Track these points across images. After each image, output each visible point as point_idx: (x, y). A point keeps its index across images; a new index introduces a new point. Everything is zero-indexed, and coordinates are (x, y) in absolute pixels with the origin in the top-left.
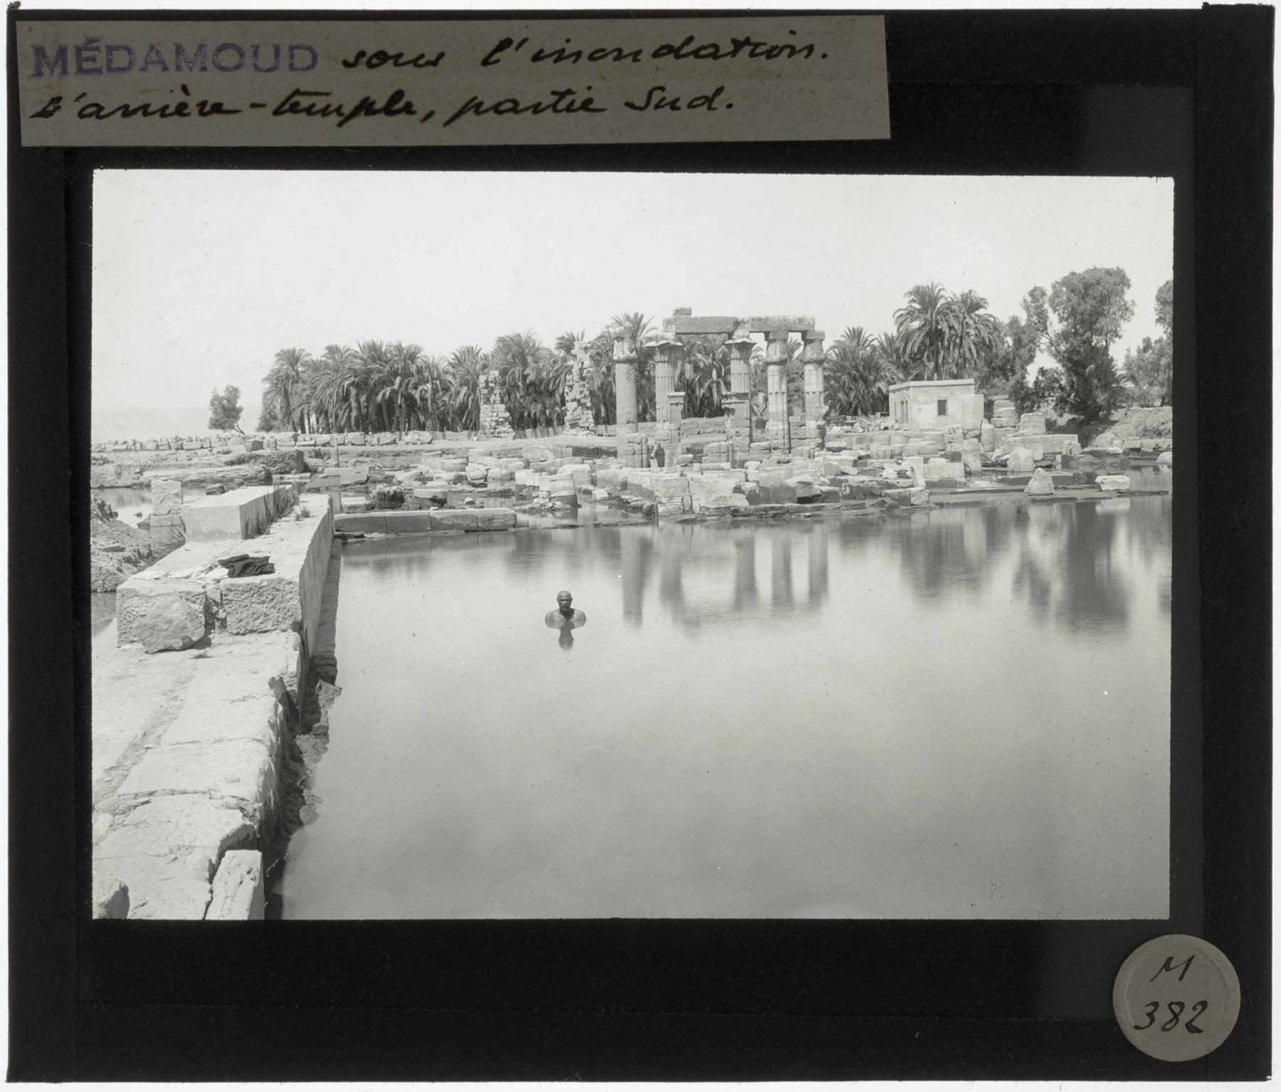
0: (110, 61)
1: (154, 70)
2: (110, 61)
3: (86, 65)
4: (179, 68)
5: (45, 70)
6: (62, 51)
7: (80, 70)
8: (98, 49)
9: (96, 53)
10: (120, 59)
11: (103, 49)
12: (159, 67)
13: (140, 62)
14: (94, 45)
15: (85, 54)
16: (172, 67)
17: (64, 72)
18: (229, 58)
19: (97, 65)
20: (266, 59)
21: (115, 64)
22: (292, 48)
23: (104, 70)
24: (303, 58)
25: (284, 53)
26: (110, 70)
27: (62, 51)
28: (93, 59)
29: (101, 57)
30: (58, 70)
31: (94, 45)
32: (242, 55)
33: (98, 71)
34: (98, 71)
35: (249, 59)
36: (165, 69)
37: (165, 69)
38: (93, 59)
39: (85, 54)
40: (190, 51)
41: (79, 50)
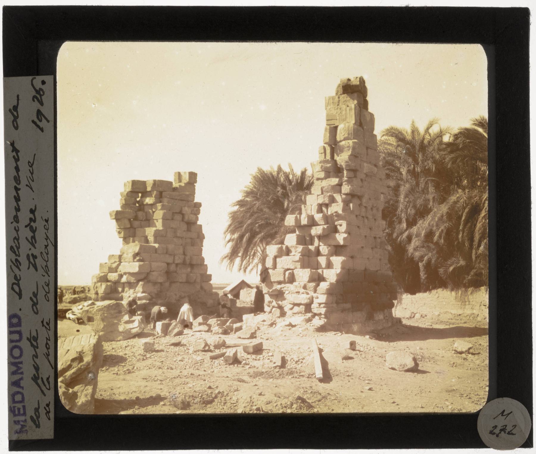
1: (22, 383)
3: (22, 411)
4: (22, 373)
7: (24, 414)
8: (14, 407)
9: (16, 408)
10: (18, 398)
11: (14, 405)
12: (21, 381)
15: (17, 412)
20: (16, 337)
21: (21, 399)
23: (23, 404)
24: (15, 321)
26: (23, 401)
28: (19, 409)
33: (24, 407)
35: (18, 344)
36: (21, 379)
37: (21, 379)
38: (19, 409)
39: (17, 412)
40: (14, 368)
41: (15, 415)
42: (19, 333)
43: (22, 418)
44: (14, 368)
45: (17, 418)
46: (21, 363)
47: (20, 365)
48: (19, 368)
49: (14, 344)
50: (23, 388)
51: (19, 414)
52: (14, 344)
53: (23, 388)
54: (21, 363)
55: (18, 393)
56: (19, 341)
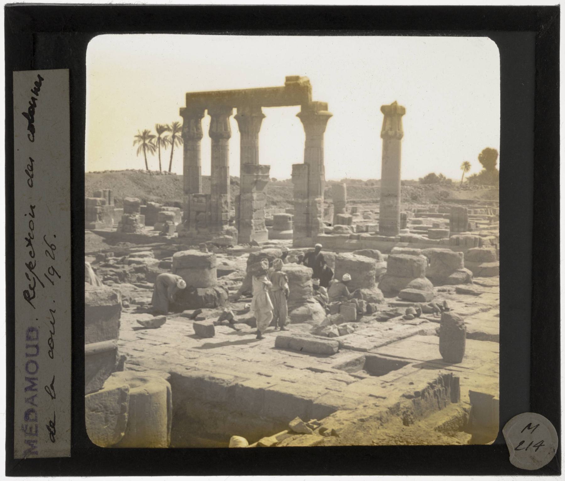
0: (33, 420)
1: (36, 401)
2: (33, 420)
3: (34, 430)
4: (36, 390)
5: (35, 450)
6: (28, 442)
8: (26, 426)
9: (28, 427)
13: (34, 407)
14: (24, 426)
16: (35, 393)
17: (35, 441)
18: (32, 367)
19: (34, 427)
21: (34, 418)
22: (28, 338)
25: (29, 343)
26: (36, 420)
27: (28, 442)
28: (31, 428)
29: (30, 424)
30: (35, 444)
31: (24, 426)
32: (32, 362)
33: (37, 427)
34: (37, 427)
35: (33, 358)
38: (31, 428)
39: (28, 431)
40: (29, 384)
42: (37, 346)
43: (35, 438)
44: (29, 384)
45: (28, 438)
46: (37, 379)
47: (35, 382)
48: (34, 384)
49: (28, 359)
50: (36, 405)
51: (31, 434)
52: (28, 359)
53: (36, 405)
54: (37, 379)
55: (32, 411)
56: (36, 355)
